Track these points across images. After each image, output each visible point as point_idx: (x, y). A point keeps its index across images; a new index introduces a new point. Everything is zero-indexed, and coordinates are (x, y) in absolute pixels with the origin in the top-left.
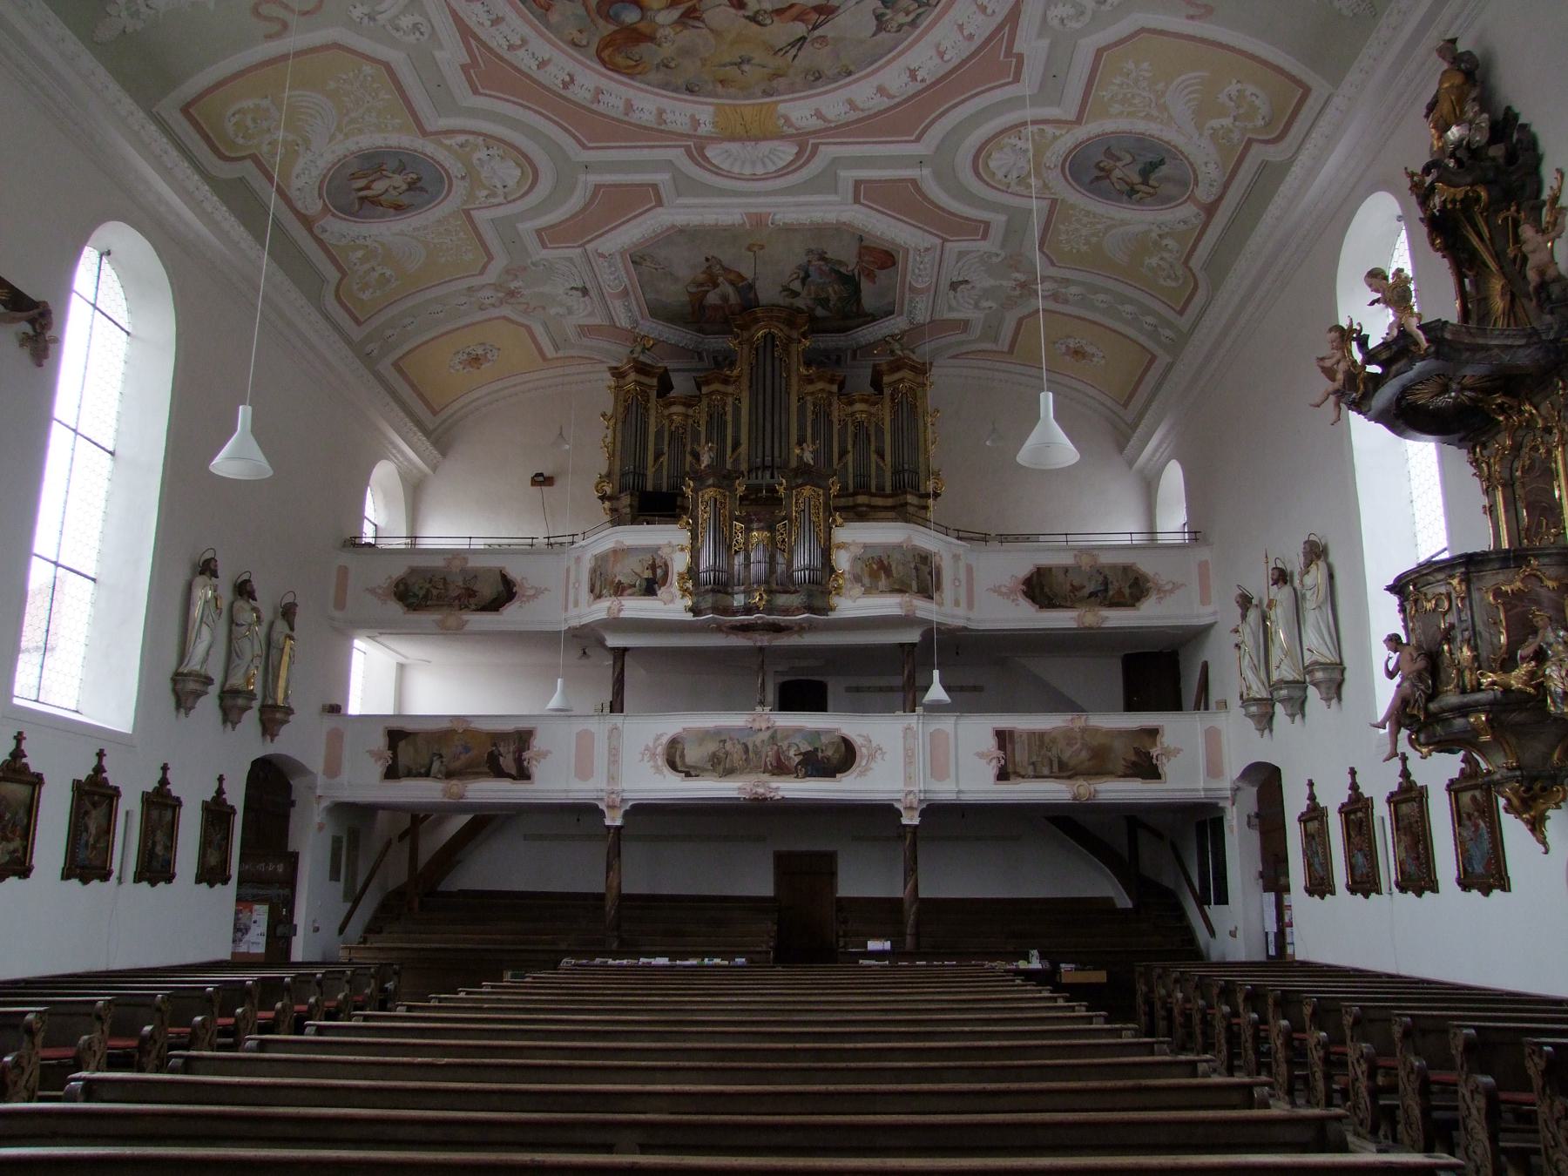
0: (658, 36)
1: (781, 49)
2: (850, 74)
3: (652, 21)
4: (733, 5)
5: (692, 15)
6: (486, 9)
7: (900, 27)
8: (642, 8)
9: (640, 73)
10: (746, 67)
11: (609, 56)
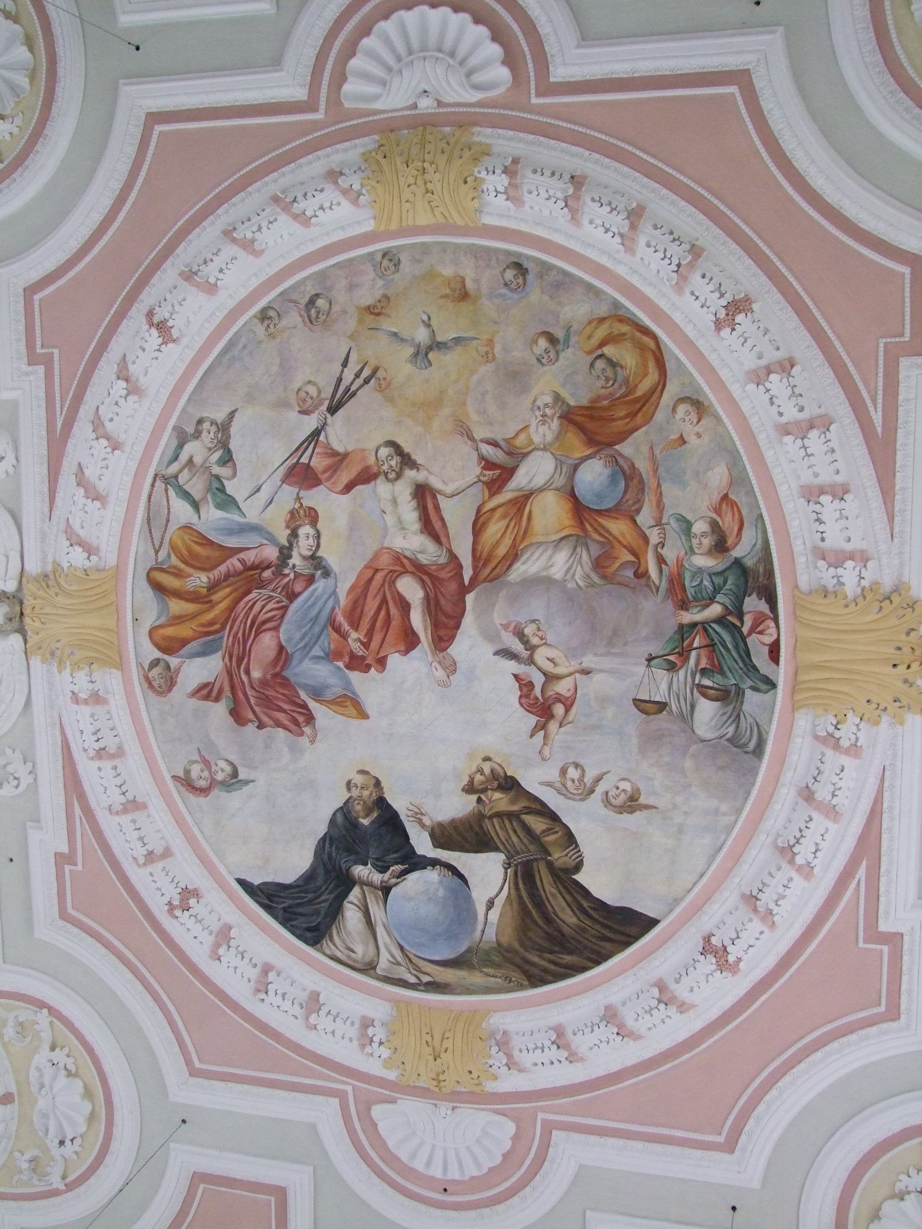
0: (555, 424)
1: (367, 381)
2: (263, 316)
3: (559, 463)
4: (434, 493)
5: (498, 472)
6: (822, 528)
7: (197, 435)
8: (572, 496)
9: (602, 320)
10: (422, 335)
11: (646, 375)
